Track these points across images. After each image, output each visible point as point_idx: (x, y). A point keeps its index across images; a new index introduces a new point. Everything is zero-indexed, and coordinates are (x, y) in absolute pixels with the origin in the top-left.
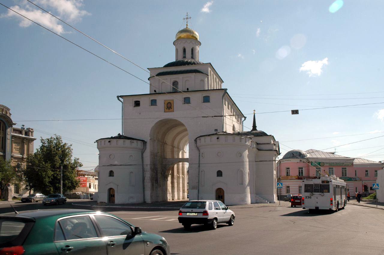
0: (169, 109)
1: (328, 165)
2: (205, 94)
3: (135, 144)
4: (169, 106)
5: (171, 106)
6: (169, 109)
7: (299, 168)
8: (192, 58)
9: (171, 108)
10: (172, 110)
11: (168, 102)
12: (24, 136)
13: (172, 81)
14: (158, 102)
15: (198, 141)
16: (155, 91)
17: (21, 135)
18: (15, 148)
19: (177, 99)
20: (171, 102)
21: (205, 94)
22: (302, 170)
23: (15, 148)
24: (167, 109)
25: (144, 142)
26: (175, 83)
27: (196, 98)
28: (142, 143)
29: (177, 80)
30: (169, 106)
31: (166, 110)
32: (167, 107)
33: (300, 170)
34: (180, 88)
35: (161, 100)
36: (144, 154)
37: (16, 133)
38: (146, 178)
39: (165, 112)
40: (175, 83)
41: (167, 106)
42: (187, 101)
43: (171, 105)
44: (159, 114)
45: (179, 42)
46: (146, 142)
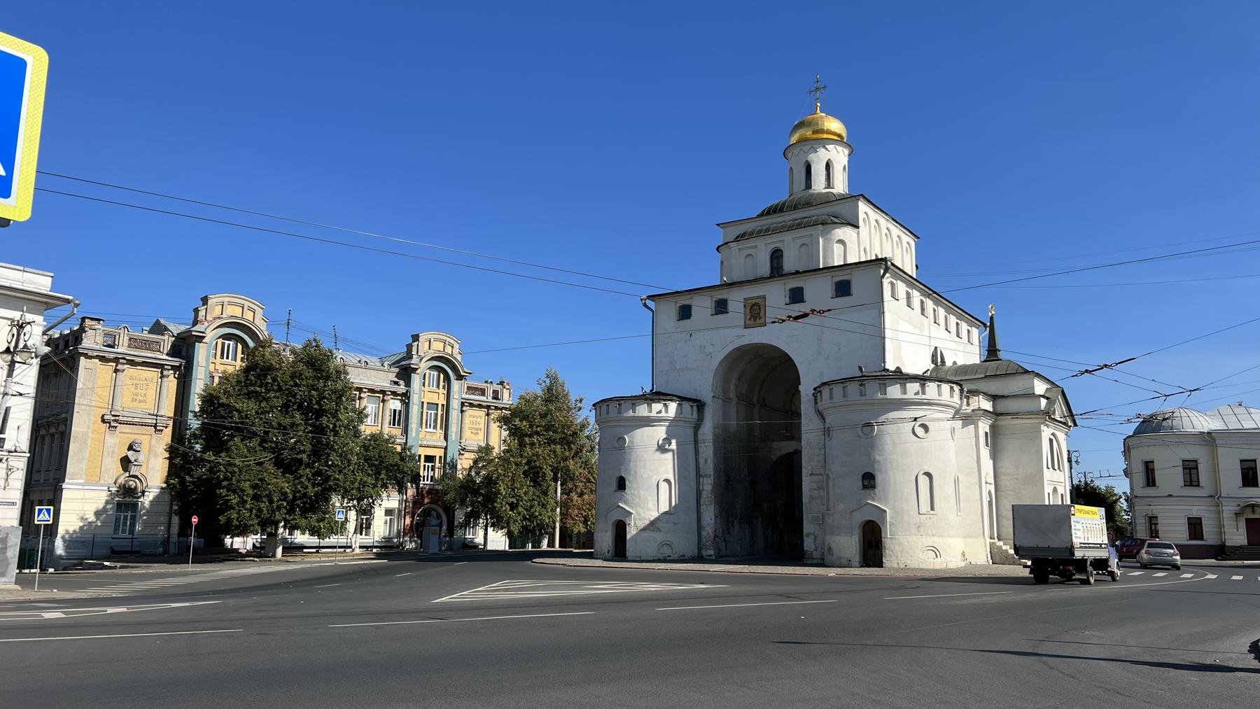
4: (755, 313)
8: (829, 185)
14: (731, 306)
17: (484, 398)
19: (775, 295)
20: (759, 301)
21: (840, 277)
25: (700, 405)
27: (818, 292)
29: (780, 245)
30: (755, 313)
34: (789, 264)
35: (736, 300)
36: (700, 432)
42: (797, 296)
44: (732, 334)
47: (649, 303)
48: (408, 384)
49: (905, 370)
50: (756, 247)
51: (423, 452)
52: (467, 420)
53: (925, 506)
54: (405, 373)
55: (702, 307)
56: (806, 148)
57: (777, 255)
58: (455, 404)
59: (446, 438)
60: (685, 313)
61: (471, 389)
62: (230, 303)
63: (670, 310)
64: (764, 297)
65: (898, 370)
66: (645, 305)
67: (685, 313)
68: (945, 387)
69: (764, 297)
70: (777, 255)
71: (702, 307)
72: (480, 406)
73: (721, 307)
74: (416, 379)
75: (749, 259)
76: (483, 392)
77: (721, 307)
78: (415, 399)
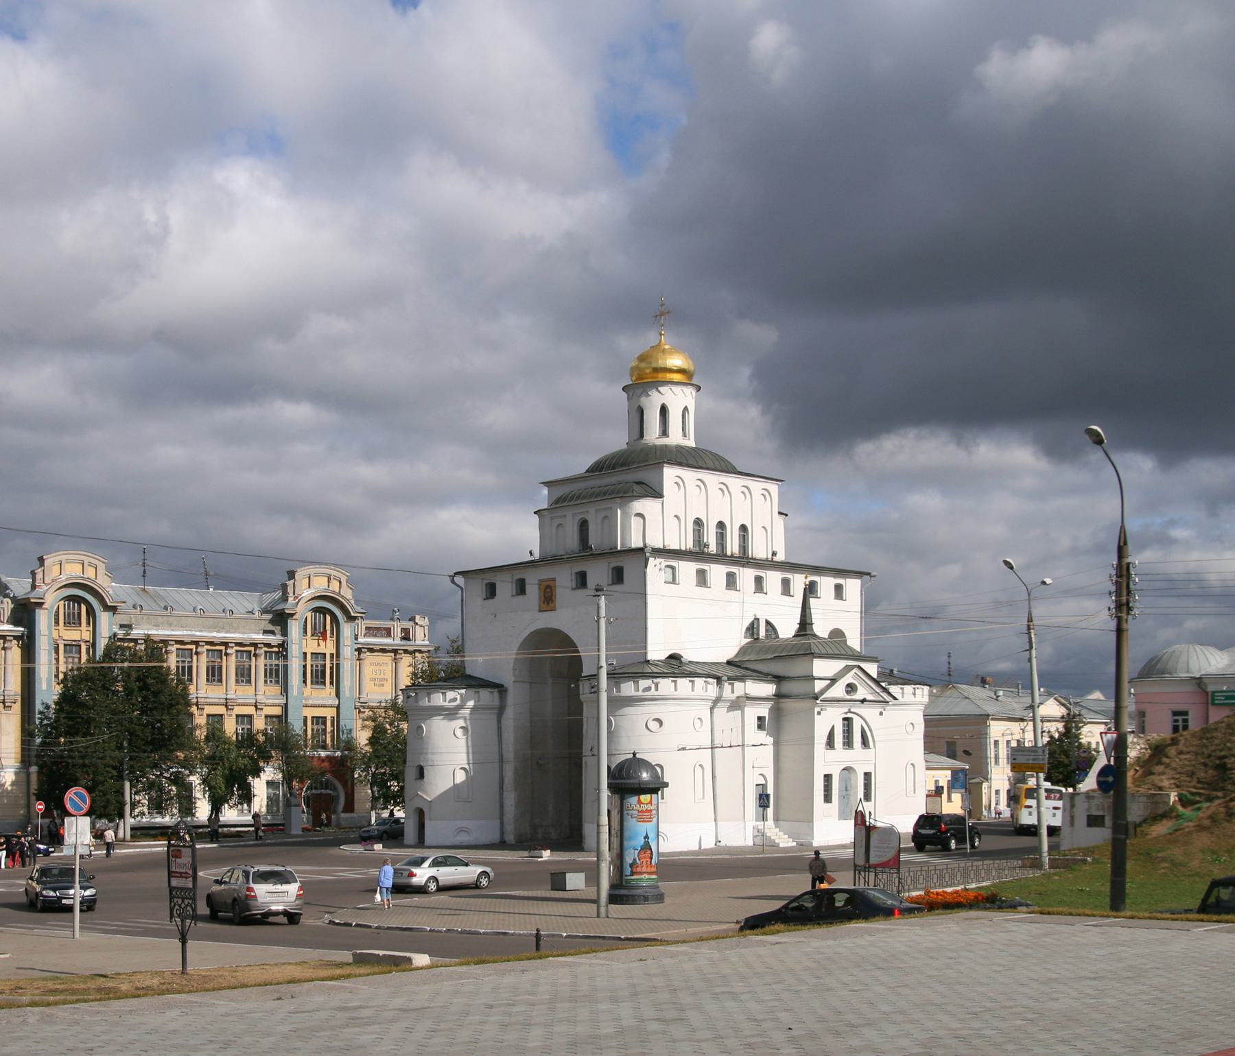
2: (615, 562)
3: (485, 693)
7: (1175, 713)
12: (398, 641)
13: (578, 518)
18: (372, 679)
19: (563, 577)
21: (615, 562)
22: (1185, 721)
23: (372, 679)
26: (584, 525)
28: (496, 694)
33: (1180, 718)
37: (375, 636)
38: (506, 781)
40: (584, 525)
46: (506, 691)
47: (457, 579)
48: (285, 632)
49: (688, 656)
51: (309, 712)
52: (368, 670)
54: (281, 619)
55: (505, 588)
56: (639, 391)
58: (347, 651)
59: (338, 695)
60: (491, 591)
61: (370, 631)
62: (68, 561)
63: (479, 589)
64: (554, 580)
65: (674, 657)
66: (453, 581)
67: (491, 591)
68: (699, 682)
69: (554, 580)
71: (505, 588)
72: (383, 651)
73: (521, 588)
74: (294, 628)
76: (388, 632)
77: (521, 588)
78: (294, 651)
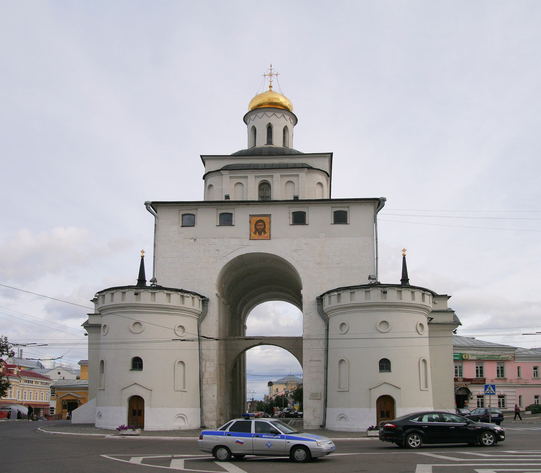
0: (260, 234)
1: (474, 358)
4: (260, 229)
5: (265, 227)
6: (260, 234)
9: (265, 233)
10: (266, 235)
11: (259, 218)
13: (259, 180)
15: (326, 299)
16: (227, 197)
24: (255, 233)
30: (260, 229)
31: (253, 235)
32: (256, 230)
39: (250, 239)
41: (255, 228)
43: (265, 225)
44: (237, 242)
45: (260, 115)
50: (246, 177)
53: (423, 387)
57: (265, 186)
70: (265, 186)
75: (239, 187)
77: (226, 220)
